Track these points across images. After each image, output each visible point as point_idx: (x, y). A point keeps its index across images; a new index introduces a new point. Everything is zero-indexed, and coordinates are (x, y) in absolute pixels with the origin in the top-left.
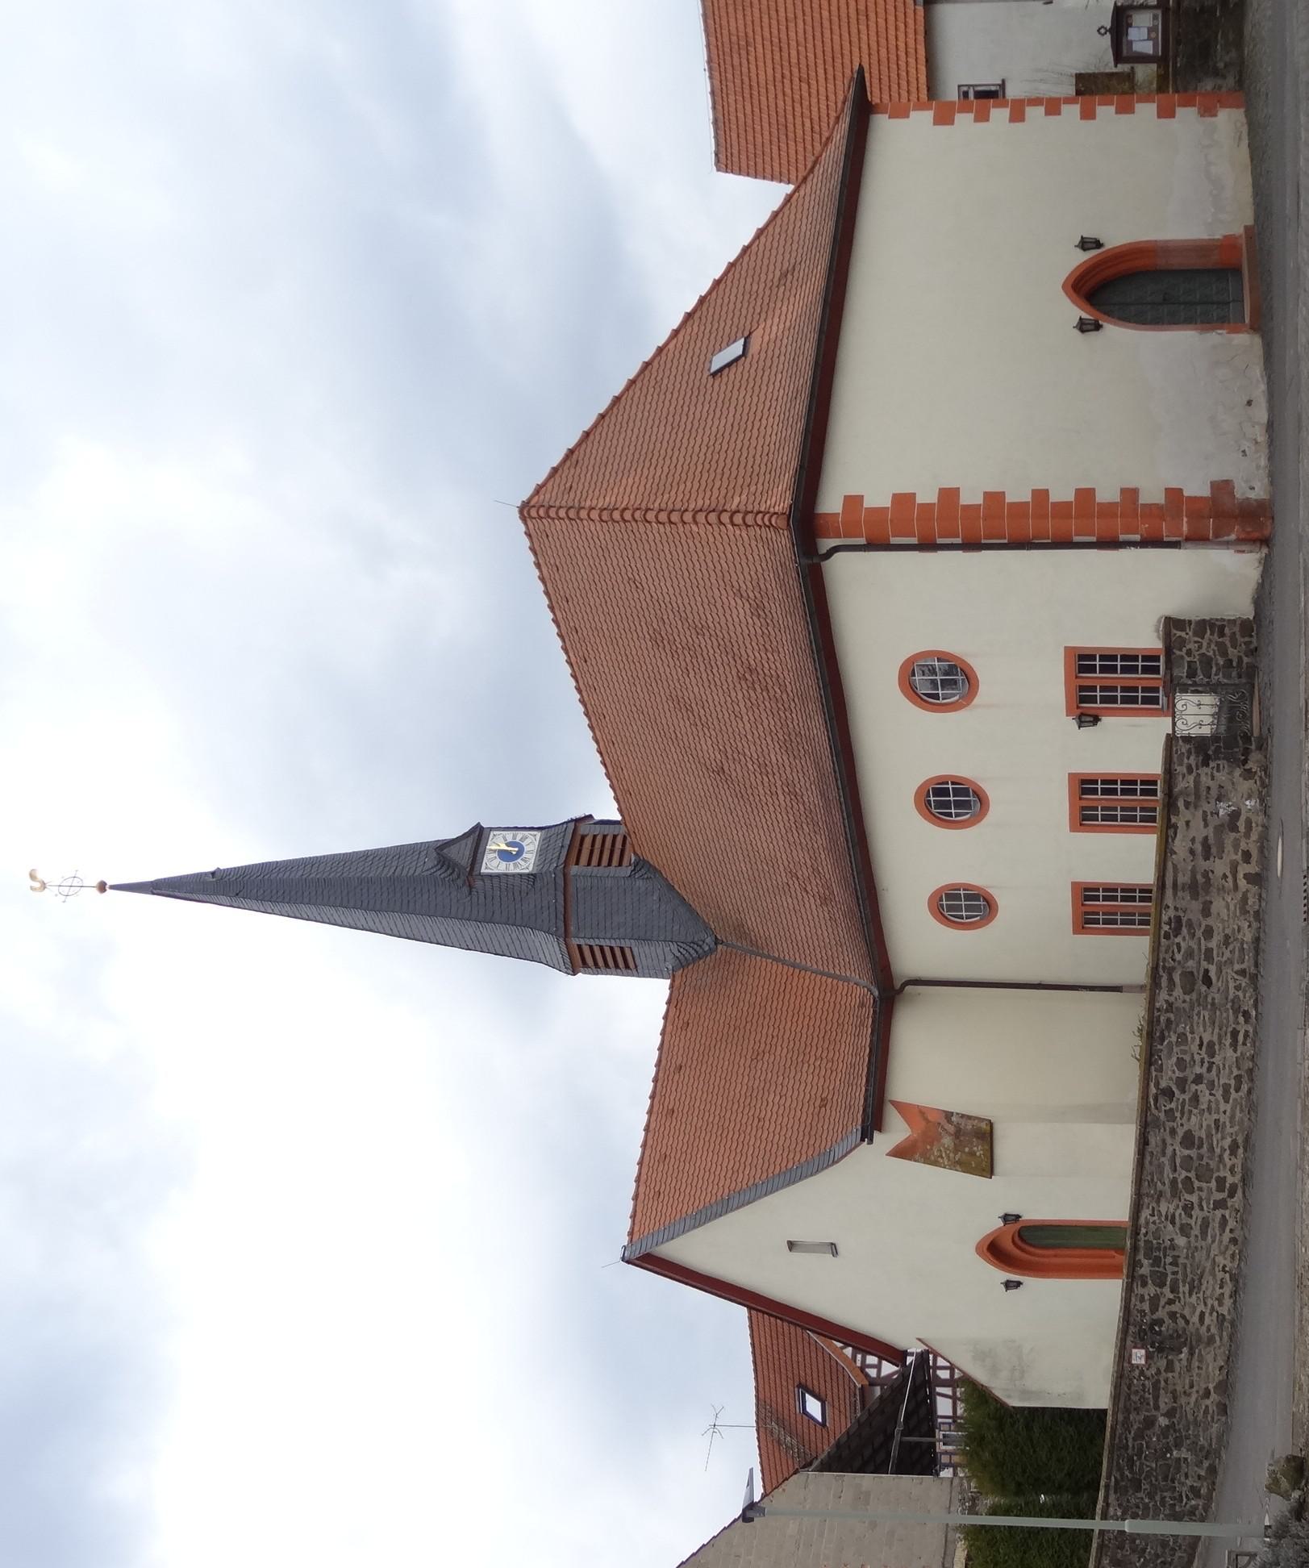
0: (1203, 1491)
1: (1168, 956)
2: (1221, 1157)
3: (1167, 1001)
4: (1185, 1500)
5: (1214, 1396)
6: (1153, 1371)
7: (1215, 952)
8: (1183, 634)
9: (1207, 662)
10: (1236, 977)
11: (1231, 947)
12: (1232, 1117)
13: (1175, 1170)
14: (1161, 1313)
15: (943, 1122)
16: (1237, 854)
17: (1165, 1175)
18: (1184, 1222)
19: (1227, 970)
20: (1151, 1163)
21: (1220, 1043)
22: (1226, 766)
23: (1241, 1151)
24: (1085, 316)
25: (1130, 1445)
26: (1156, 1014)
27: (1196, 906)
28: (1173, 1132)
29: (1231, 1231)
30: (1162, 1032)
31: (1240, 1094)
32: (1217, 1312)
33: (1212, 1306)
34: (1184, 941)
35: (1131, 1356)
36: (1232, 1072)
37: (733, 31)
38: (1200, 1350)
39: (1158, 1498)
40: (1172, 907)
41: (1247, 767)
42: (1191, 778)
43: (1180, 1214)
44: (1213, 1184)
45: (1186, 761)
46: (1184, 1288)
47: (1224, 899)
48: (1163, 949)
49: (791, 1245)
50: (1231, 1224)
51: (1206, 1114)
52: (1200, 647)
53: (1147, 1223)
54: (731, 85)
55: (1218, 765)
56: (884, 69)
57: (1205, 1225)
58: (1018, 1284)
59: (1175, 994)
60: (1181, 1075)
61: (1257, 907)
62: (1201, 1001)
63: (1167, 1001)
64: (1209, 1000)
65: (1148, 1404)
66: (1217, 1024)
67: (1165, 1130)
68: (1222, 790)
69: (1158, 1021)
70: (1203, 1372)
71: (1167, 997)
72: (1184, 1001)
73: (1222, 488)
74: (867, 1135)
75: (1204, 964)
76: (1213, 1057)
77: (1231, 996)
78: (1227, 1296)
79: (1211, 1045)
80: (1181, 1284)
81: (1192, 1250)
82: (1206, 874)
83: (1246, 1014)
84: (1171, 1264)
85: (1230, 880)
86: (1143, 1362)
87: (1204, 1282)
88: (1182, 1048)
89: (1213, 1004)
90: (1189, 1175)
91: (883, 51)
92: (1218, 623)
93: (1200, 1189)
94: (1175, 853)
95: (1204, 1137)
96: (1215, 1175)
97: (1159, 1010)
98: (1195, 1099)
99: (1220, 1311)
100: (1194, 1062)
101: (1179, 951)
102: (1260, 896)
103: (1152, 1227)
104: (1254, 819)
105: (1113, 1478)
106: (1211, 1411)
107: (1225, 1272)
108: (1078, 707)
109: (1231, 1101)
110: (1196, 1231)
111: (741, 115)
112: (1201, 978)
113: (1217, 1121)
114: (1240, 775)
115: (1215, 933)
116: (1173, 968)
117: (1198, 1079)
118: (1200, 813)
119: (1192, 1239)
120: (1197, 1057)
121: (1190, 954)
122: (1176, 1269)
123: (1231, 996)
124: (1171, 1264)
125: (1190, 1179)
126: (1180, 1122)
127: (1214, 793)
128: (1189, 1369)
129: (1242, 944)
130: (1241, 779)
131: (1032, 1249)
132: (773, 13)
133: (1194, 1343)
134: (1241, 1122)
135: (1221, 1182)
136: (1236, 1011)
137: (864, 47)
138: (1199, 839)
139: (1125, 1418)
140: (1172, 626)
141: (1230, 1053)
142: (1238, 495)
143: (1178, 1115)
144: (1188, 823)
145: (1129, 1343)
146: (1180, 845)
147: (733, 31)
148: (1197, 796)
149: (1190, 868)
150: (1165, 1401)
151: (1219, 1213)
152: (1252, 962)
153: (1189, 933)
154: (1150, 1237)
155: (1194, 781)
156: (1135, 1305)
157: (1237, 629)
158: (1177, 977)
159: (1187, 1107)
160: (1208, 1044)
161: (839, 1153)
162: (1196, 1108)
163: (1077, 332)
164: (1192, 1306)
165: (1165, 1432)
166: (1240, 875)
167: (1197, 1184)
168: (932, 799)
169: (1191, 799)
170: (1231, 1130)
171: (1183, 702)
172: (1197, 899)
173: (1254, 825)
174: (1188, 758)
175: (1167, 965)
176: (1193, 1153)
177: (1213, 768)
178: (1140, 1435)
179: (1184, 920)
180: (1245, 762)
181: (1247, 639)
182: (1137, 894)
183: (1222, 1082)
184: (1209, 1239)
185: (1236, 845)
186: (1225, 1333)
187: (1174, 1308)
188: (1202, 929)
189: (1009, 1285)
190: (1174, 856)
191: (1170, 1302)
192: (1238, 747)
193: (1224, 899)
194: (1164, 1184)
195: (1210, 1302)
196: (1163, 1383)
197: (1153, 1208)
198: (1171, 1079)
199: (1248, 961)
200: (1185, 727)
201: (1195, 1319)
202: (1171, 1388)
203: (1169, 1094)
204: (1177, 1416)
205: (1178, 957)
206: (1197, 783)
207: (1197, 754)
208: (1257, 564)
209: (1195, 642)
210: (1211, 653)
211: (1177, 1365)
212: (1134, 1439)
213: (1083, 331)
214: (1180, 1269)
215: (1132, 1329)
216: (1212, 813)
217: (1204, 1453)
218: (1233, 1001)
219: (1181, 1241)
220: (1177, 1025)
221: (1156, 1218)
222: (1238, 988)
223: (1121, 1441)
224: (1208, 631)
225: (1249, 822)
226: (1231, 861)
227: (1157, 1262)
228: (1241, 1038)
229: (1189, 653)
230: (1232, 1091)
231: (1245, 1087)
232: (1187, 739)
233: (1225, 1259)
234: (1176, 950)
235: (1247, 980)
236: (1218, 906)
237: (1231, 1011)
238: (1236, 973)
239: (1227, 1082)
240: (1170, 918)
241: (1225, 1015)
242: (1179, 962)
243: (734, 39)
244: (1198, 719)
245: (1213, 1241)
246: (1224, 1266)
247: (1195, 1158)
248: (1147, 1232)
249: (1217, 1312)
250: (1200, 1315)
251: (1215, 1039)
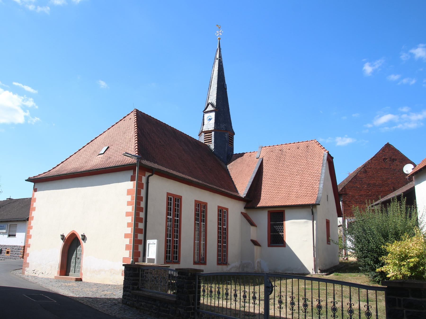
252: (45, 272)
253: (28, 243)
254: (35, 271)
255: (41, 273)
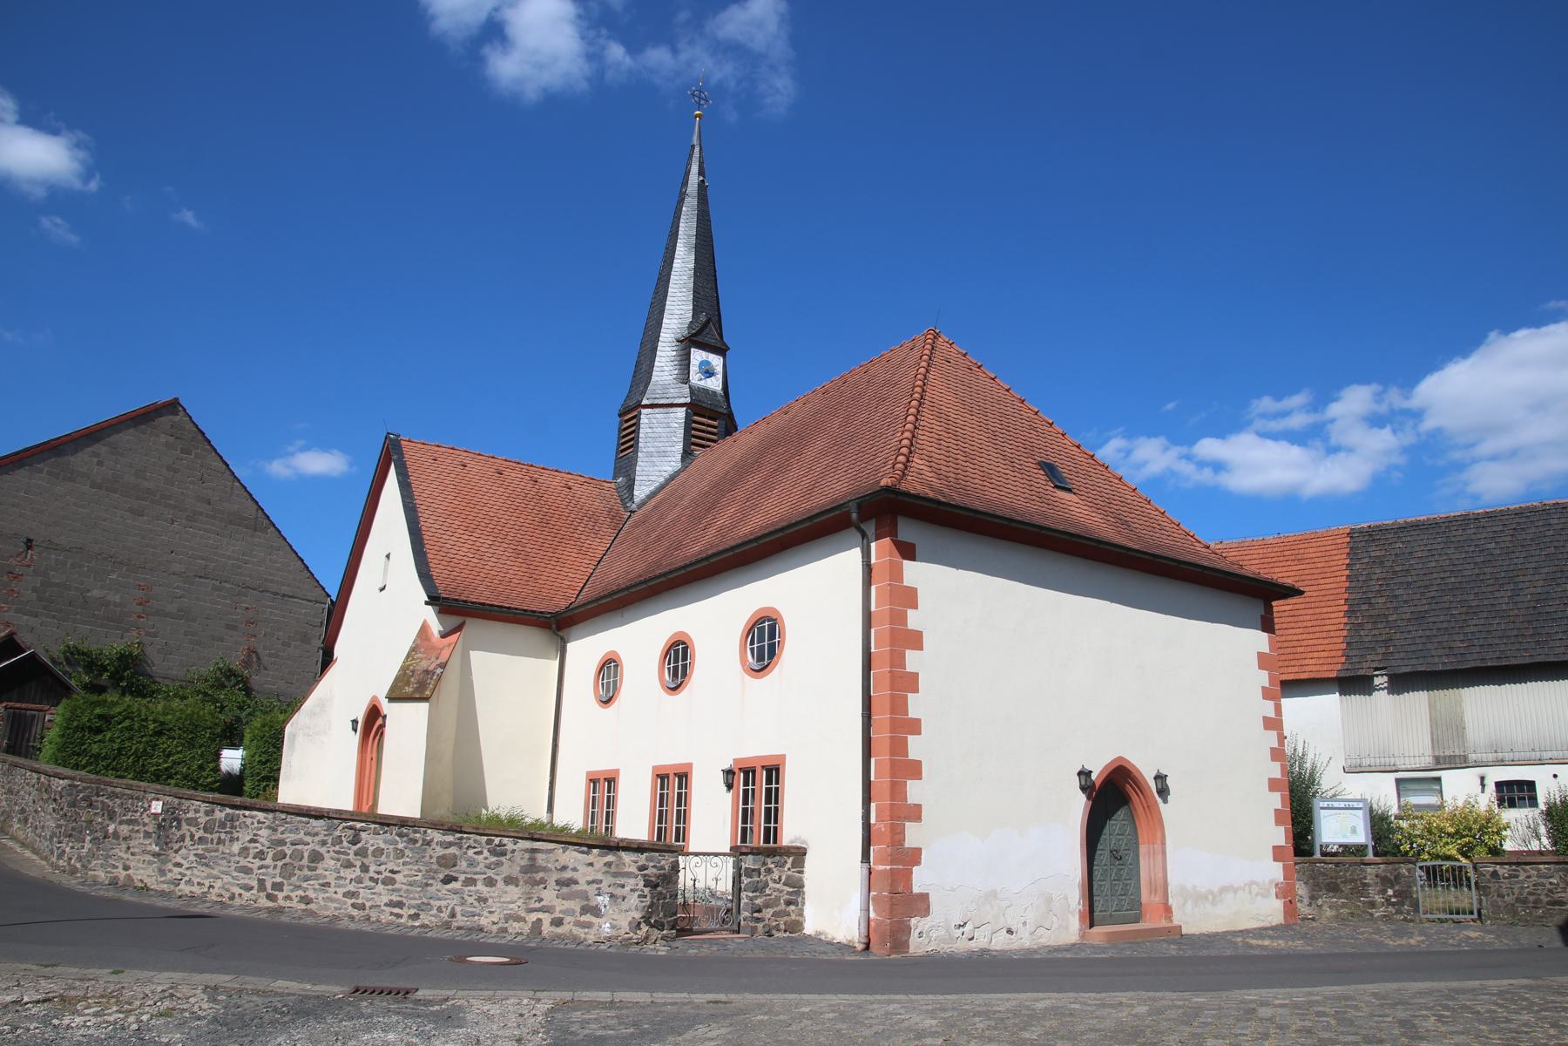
0: (61, 863)
1: (471, 842)
2: (299, 887)
3: (432, 840)
4: (58, 845)
5: (124, 873)
6: (146, 820)
7: (472, 888)
8: (788, 865)
9: (759, 888)
10: (449, 908)
11: (476, 903)
12: (330, 899)
13: (293, 844)
14: (185, 826)
15: (438, 662)
16: (560, 912)
17: (289, 835)
18: (251, 851)
19: (456, 900)
20: (301, 822)
21: (393, 890)
22: (644, 904)
23: (303, 906)
24: (1094, 777)
25: (100, 798)
26: (422, 829)
27: (516, 871)
28: (324, 843)
29: (240, 895)
30: (407, 835)
31: (350, 908)
32: (181, 880)
33: (184, 875)
34: (486, 857)
35: (158, 800)
36: (368, 900)
37: (1307, 551)
38: (155, 862)
39: (62, 822)
40: (515, 847)
41: (643, 925)
42: (633, 869)
43: (257, 848)
44: (279, 880)
45: (652, 864)
46: (200, 849)
47: (520, 898)
48: (478, 837)
49: (388, 556)
50: (247, 895)
51: (336, 875)
52: (775, 881)
53: (252, 817)
54: (1269, 550)
55: (645, 897)
56: (1289, 650)
57: (247, 871)
58: (355, 730)
59: (438, 848)
60: (369, 852)
61: (510, 930)
62: (430, 874)
63: (432, 840)
64: (431, 881)
65: (124, 815)
66: (409, 887)
67: (325, 835)
68: (620, 900)
69: (415, 832)
70: (141, 865)
71: (436, 840)
72: (431, 857)
73: (921, 904)
74: (433, 600)
75: (462, 877)
76: (383, 883)
77: (432, 902)
78: (193, 889)
79: (393, 882)
80: (203, 847)
81: (227, 857)
82: (543, 881)
83: (415, 916)
84: (219, 838)
85: (537, 905)
86: (153, 811)
87: (203, 868)
88: (392, 854)
89: (427, 885)
90: (288, 856)
91: (1302, 649)
92: (800, 900)
93: (275, 867)
94: (564, 852)
95: (318, 872)
96: (285, 882)
97: (425, 832)
98: (349, 865)
99: (183, 882)
100: (379, 865)
101: (475, 853)
102: (521, 934)
103: (249, 821)
104: (593, 931)
105: (79, 783)
106: (113, 871)
107: (209, 888)
108: (740, 769)
109: (346, 899)
110: (243, 862)
111: (1249, 557)
112: (451, 873)
113: (328, 885)
114: (634, 918)
115: (488, 889)
116: (461, 848)
117: (365, 869)
118: (600, 876)
119: (237, 858)
120: (383, 867)
121: (472, 864)
122: (215, 843)
123: (432, 902)
124: (219, 838)
125: (284, 858)
126: (331, 850)
127: (619, 892)
128: (144, 852)
129: (479, 915)
130: (630, 919)
131: (378, 737)
132: (1322, 575)
133: (162, 857)
134: (326, 908)
135: (278, 887)
136: (418, 907)
137: (1304, 636)
138: (575, 875)
139: (117, 794)
140: (798, 854)
141: (385, 899)
142: (913, 921)
143: (337, 848)
144: (591, 864)
145: (169, 799)
146: (571, 857)
147: (1307, 551)
148: (616, 875)
149: (549, 865)
150: (124, 830)
151: (255, 883)
152: (461, 924)
153: (490, 864)
154: (242, 819)
155: (631, 873)
156: (193, 805)
157: (793, 917)
158: (453, 850)
159: (343, 857)
160: (394, 879)
161: (251, 509)
162: (341, 866)
163: (1079, 768)
164: (186, 856)
165: (104, 829)
166: (540, 915)
167: (280, 864)
168: (681, 646)
169: (613, 869)
170: (320, 898)
171: (720, 863)
172: (521, 872)
173: (586, 930)
174: (654, 867)
175: (464, 841)
176: (305, 861)
177: (642, 891)
178: (104, 806)
179: (503, 859)
180: (647, 922)
181: (782, 927)
182: (663, 825)
183: (361, 891)
184: (235, 874)
185: (571, 913)
186: (165, 886)
187: (188, 839)
188: (493, 876)
189: (355, 722)
190: (561, 850)
191: (192, 836)
192: (665, 916)
193: (520, 898)
194: (282, 833)
195: (188, 872)
196: (137, 828)
197: (264, 823)
198: (367, 842)
199: (463, 921)
200: (693, 864)
201: (179, 859)
202: (133, 835)
203: (355, 841)
204: (114, 841)
205: (471, 852)
206: (629, 875)
207: (658, 877)
208: (849, 938)
209: (780, 877)
210: (768, 892)
211: (147, 842)
212: (102, 802)
213: (1080, 774)
214: (214, 846)
215: (176, 801)
216: (599, 889)
217: (86, 863)
218: (429, 904)
219: (236, 848)
220: (411, 849)
221: (256, 825)
222: (440, 909)
223: (102, 790)
224: (791, 890)
225: (589, 925)
226: (555, 906)
227: (223, 825)
228: (396, 910)
229: (769, 871)
230: (353, 901)
231: (355, 912)
232: (675, 868)
233: (219, 888)
234: (476, 850)
235: (446, 918)
236: (514, 892)
237: (419, 902)
238: (453, 908)
239: (361, 896)
240: (505, 845)
241: (417, 895)
242: (465, 853)
243: (1302, 551)
244: (701, 877)
245: (233, 877)
246: (213, 887)
247: (301, 863)
248: (245, 817)
249: (181, 880)
250: (179, 864)
251: (397, 886)
252: (1025, 923)
253: (906, 798)
254: (967, 929)
255: (1004, 931)
